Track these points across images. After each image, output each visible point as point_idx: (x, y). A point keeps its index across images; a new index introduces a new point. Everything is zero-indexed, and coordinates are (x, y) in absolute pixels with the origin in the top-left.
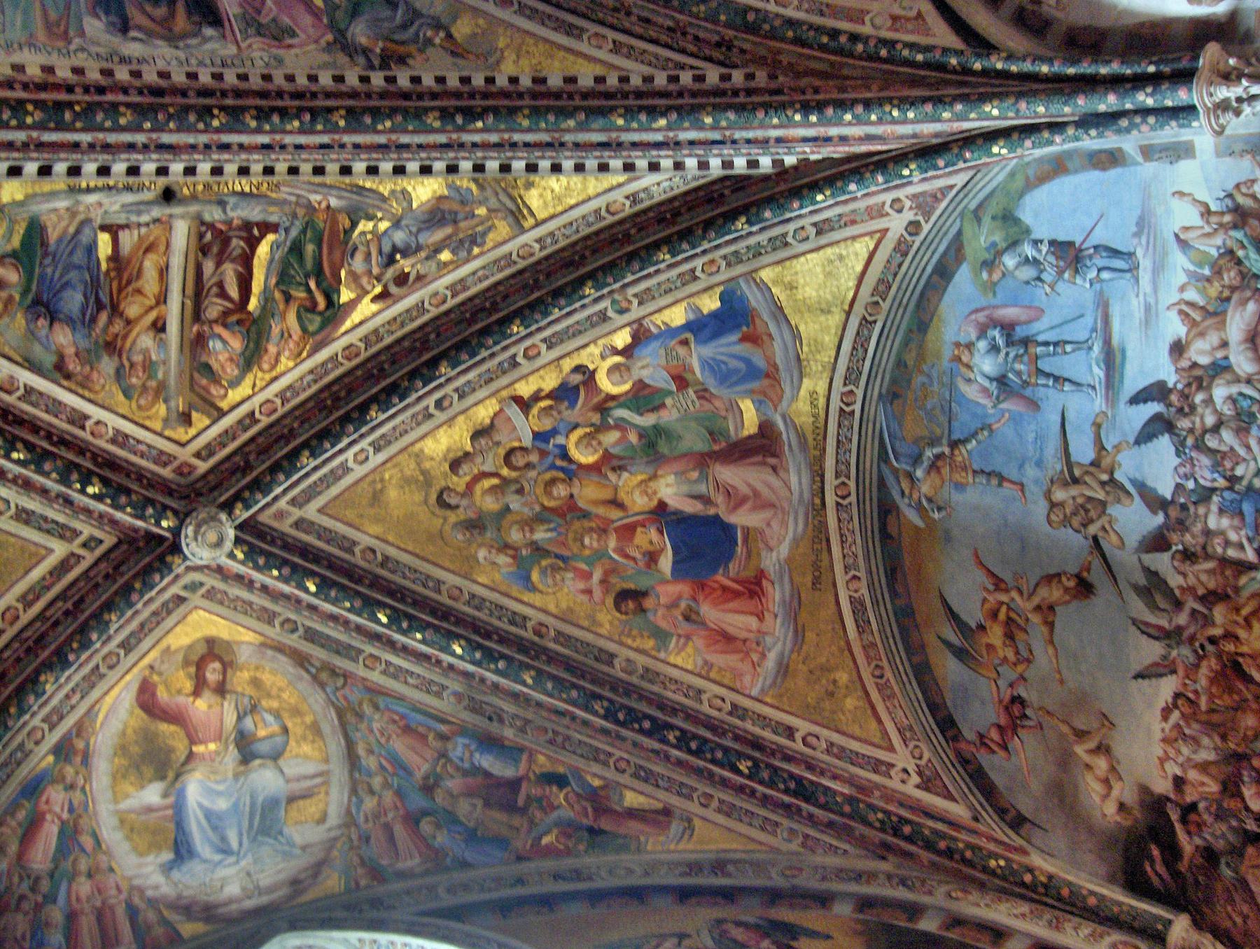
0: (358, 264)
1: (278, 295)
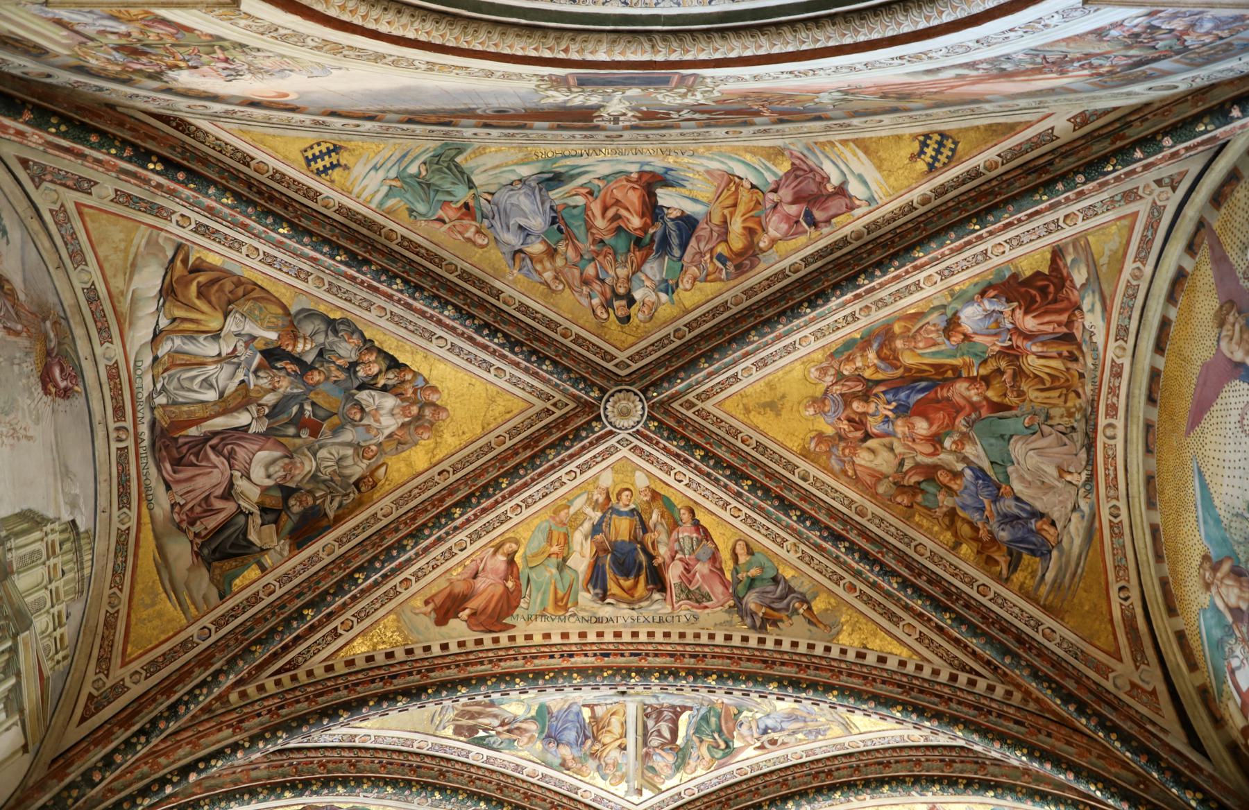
0: (744, 730)
1: (694, 738)
